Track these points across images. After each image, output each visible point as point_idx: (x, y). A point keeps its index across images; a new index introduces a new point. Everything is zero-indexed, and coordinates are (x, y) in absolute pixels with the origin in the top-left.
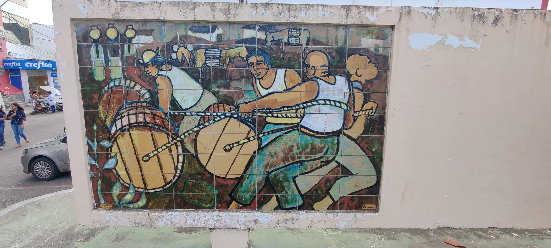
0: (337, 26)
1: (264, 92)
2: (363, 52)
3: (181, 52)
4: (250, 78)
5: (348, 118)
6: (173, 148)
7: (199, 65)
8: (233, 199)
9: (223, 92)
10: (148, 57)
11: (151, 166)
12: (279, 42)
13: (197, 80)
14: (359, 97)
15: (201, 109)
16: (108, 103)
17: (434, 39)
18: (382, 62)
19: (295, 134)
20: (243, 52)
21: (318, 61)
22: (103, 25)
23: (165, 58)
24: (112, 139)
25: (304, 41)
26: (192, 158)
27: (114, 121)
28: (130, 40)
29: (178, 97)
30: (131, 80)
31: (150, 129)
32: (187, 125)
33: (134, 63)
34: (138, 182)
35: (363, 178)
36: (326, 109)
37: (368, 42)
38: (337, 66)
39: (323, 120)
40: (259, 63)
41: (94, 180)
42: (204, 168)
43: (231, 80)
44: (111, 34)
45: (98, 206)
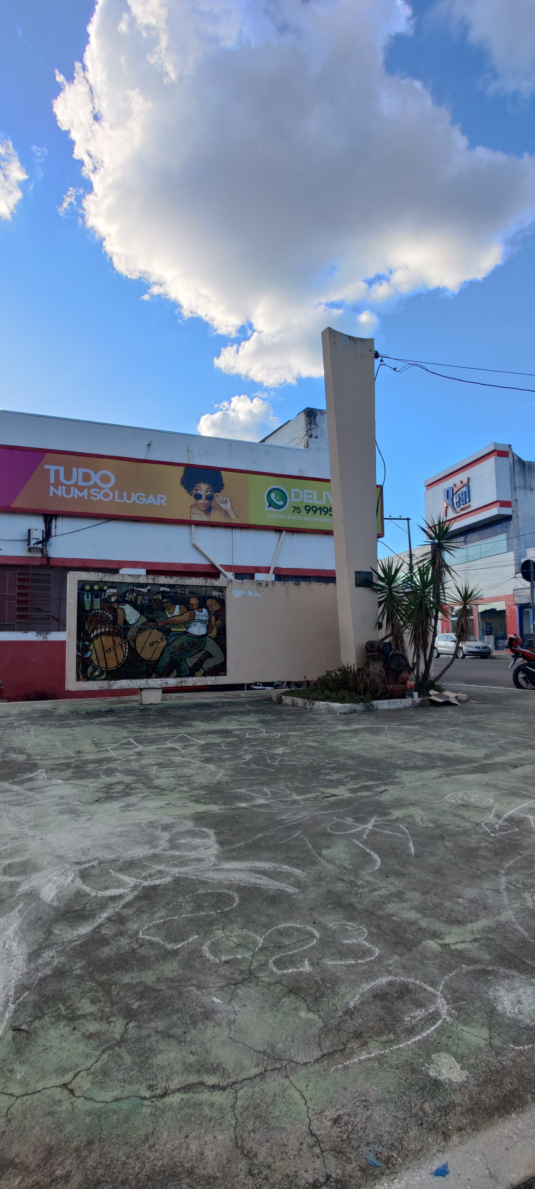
0: (202, 586)
1: (170, 616)
2: (214, 598)
3: (129, 597)
4: (163, 610)
5: (209, 628)
6: (124, 645)
7: (139, 603)
8: (154, 672)
9: (150, 616)
10: (113, 599)
11: (111, 655)
12: (177, 593)
13: (137, 610)
14: (213, 618)
15: (139, 624)
16: (91, 621)
17: (243, 593)
18: (222, 602)
19: (184, 637)
20: (160, 597)
21: (194, 601)
22: (92, 583)
23: (122, 599)
24: (91, 641)
25: (187, 593)
26: (133, 650)
27: (93, 631)
28: (105, 591)
29: (128, 618)
30: (104, 610)
31: (112, 635)
32: (130, 633)
33: (106, 602)
34: (103, 664)
35: (218, 660)
36: (199, 624)
37: (215, 593)
38: (202, 605)
39: (197, 630)
40: (167, 602)
41: (78, 664)
42: (139, 655)
43: (154, 610)
44: (96, 587)
45: (78, 679)
